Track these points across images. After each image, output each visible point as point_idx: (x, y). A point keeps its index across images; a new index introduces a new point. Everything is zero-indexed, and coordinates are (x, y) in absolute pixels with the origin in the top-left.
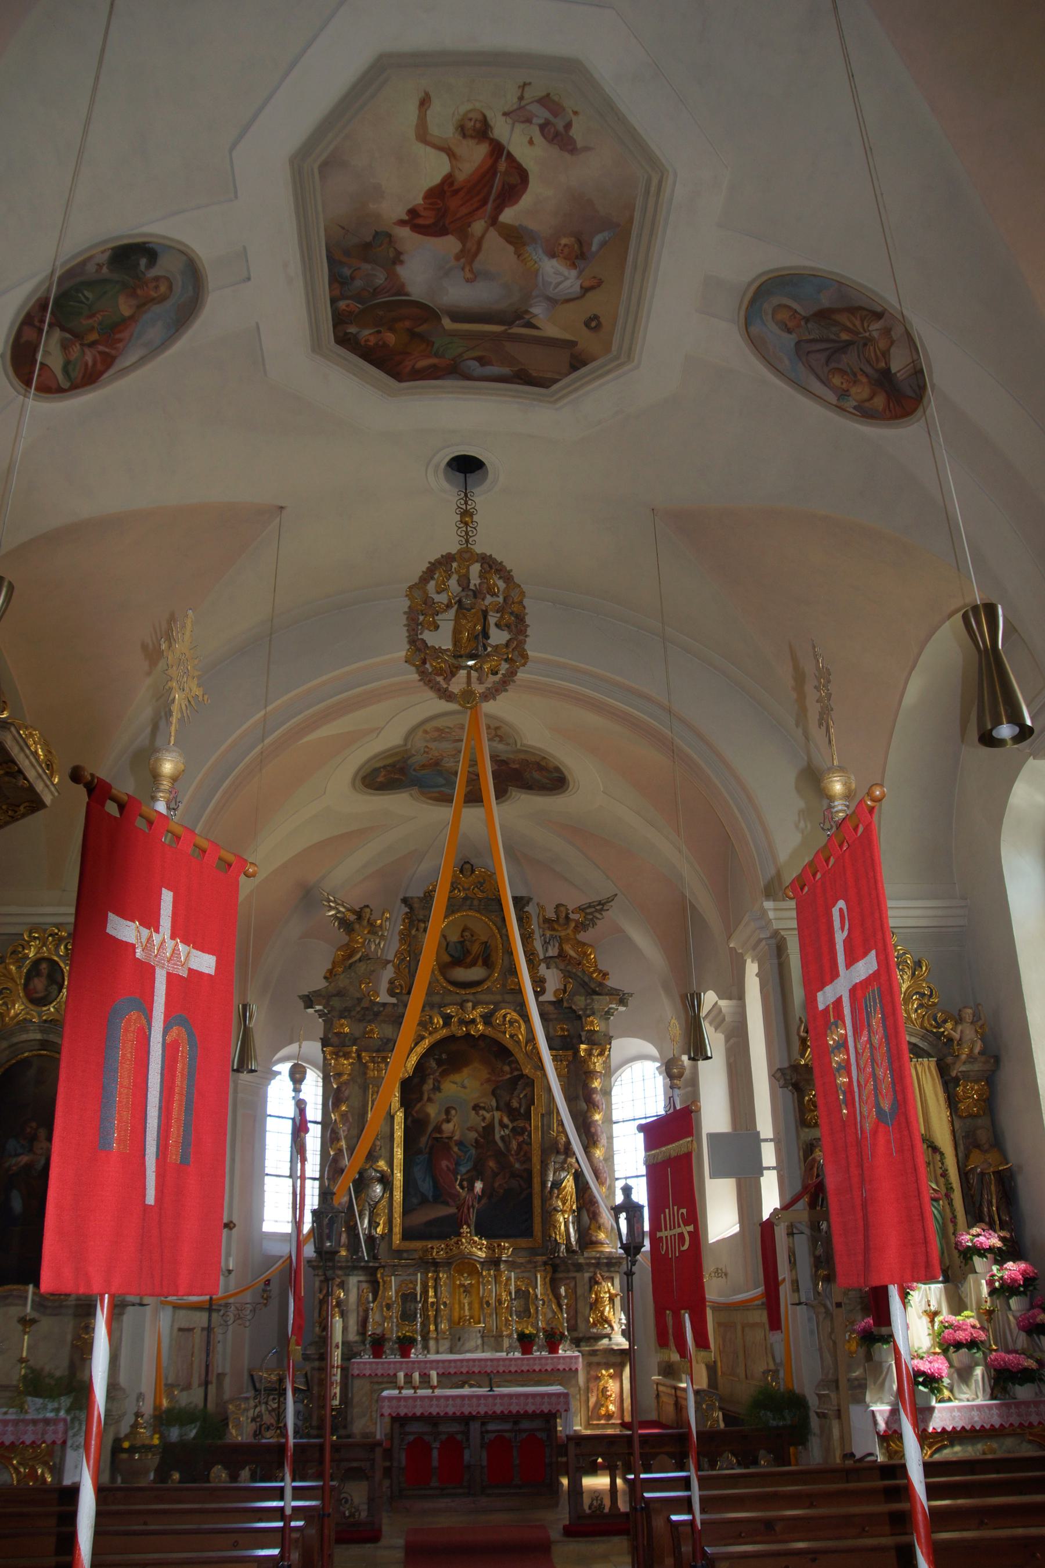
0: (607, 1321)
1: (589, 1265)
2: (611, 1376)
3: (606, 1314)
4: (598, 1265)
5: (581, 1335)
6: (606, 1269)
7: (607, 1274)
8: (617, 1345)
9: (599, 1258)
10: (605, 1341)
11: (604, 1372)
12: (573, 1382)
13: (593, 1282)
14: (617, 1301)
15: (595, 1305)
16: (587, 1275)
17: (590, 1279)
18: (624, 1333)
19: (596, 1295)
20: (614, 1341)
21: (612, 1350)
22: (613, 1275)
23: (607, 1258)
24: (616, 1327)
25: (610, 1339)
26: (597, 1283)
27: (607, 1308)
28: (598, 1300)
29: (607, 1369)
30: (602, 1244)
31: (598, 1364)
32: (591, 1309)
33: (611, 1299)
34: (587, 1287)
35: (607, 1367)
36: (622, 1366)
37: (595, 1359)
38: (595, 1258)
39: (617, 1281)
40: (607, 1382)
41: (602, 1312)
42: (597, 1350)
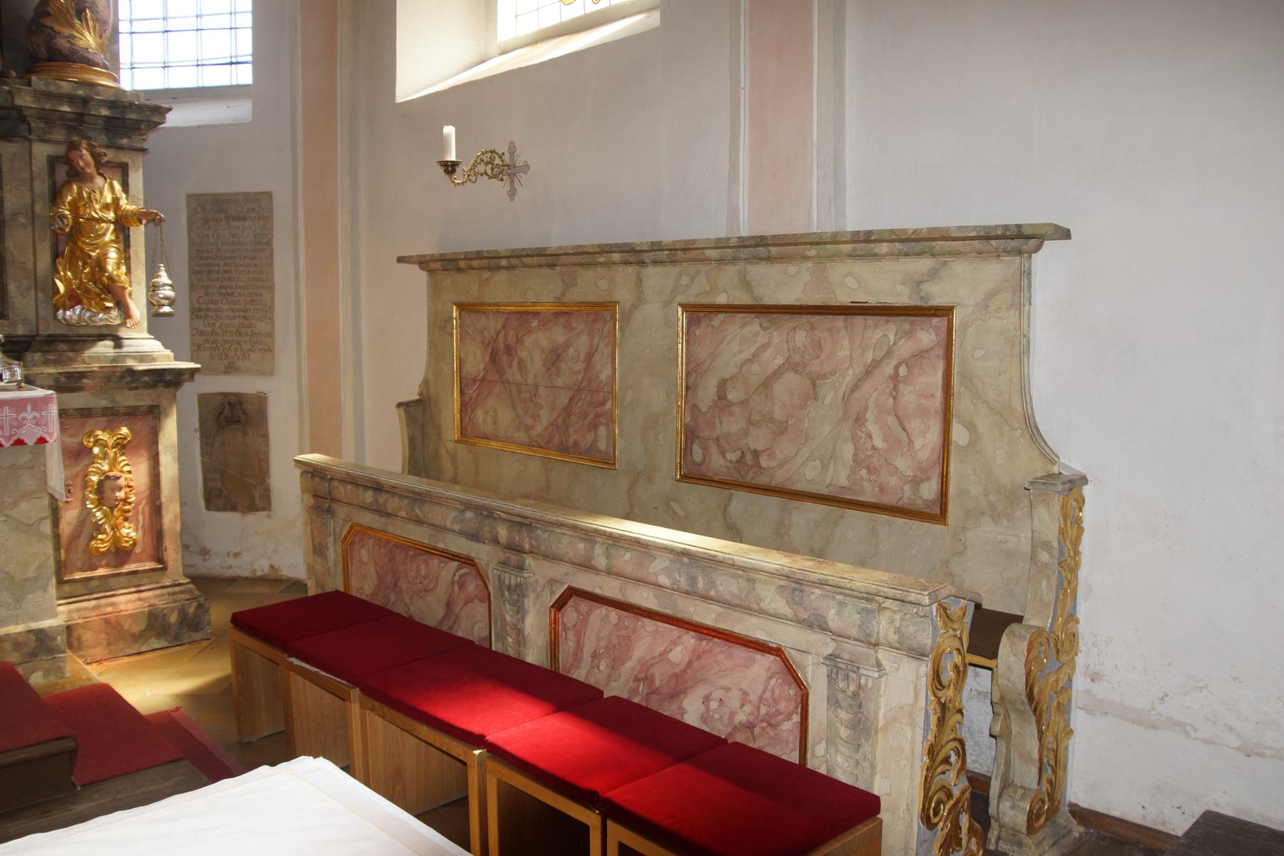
0: (113, 293)
1: (50, 118)
2: (122, 446)
3: (110, 267)
4: (78, 123)
5: (21, 331)
6: (103, 138)
7: (110, 155)
8: (142, 358)
9: (85, 101)
10: (104, 348)
11: (102, 435)
12: (28, 482)
13: (66, 172)
14: (138, 234)
15: (70, 242)
16: (41, 151)
17: (53, 161)
18: (157, 323)
19: (74, 208)
20: (130, 346)
21: (131, 371)
22: (124, 158)
23: (112, 104)
24: (138, 308)
25: (118, 343)
26: (77, 175)
27: (113, 254)
28: (80, 230)
29: (111, 428)
30: (90, 63)
31: (86, 413)
32: (56, 254)
33: (122, 226)
34: (42, 187)
35: (112, 416)
36: (154, 414)
37: (77, 400)
38: (71, 99)
39: (137, 179)
40: (114, 464)
41: (100, 264)
42: (83, 375)
